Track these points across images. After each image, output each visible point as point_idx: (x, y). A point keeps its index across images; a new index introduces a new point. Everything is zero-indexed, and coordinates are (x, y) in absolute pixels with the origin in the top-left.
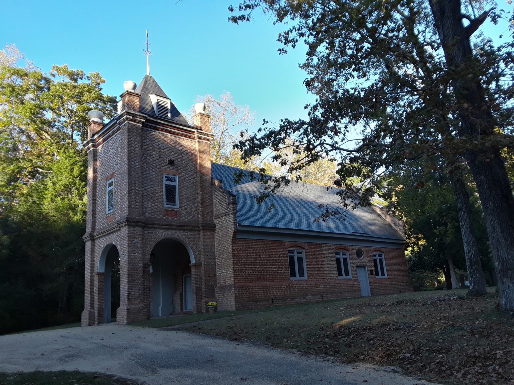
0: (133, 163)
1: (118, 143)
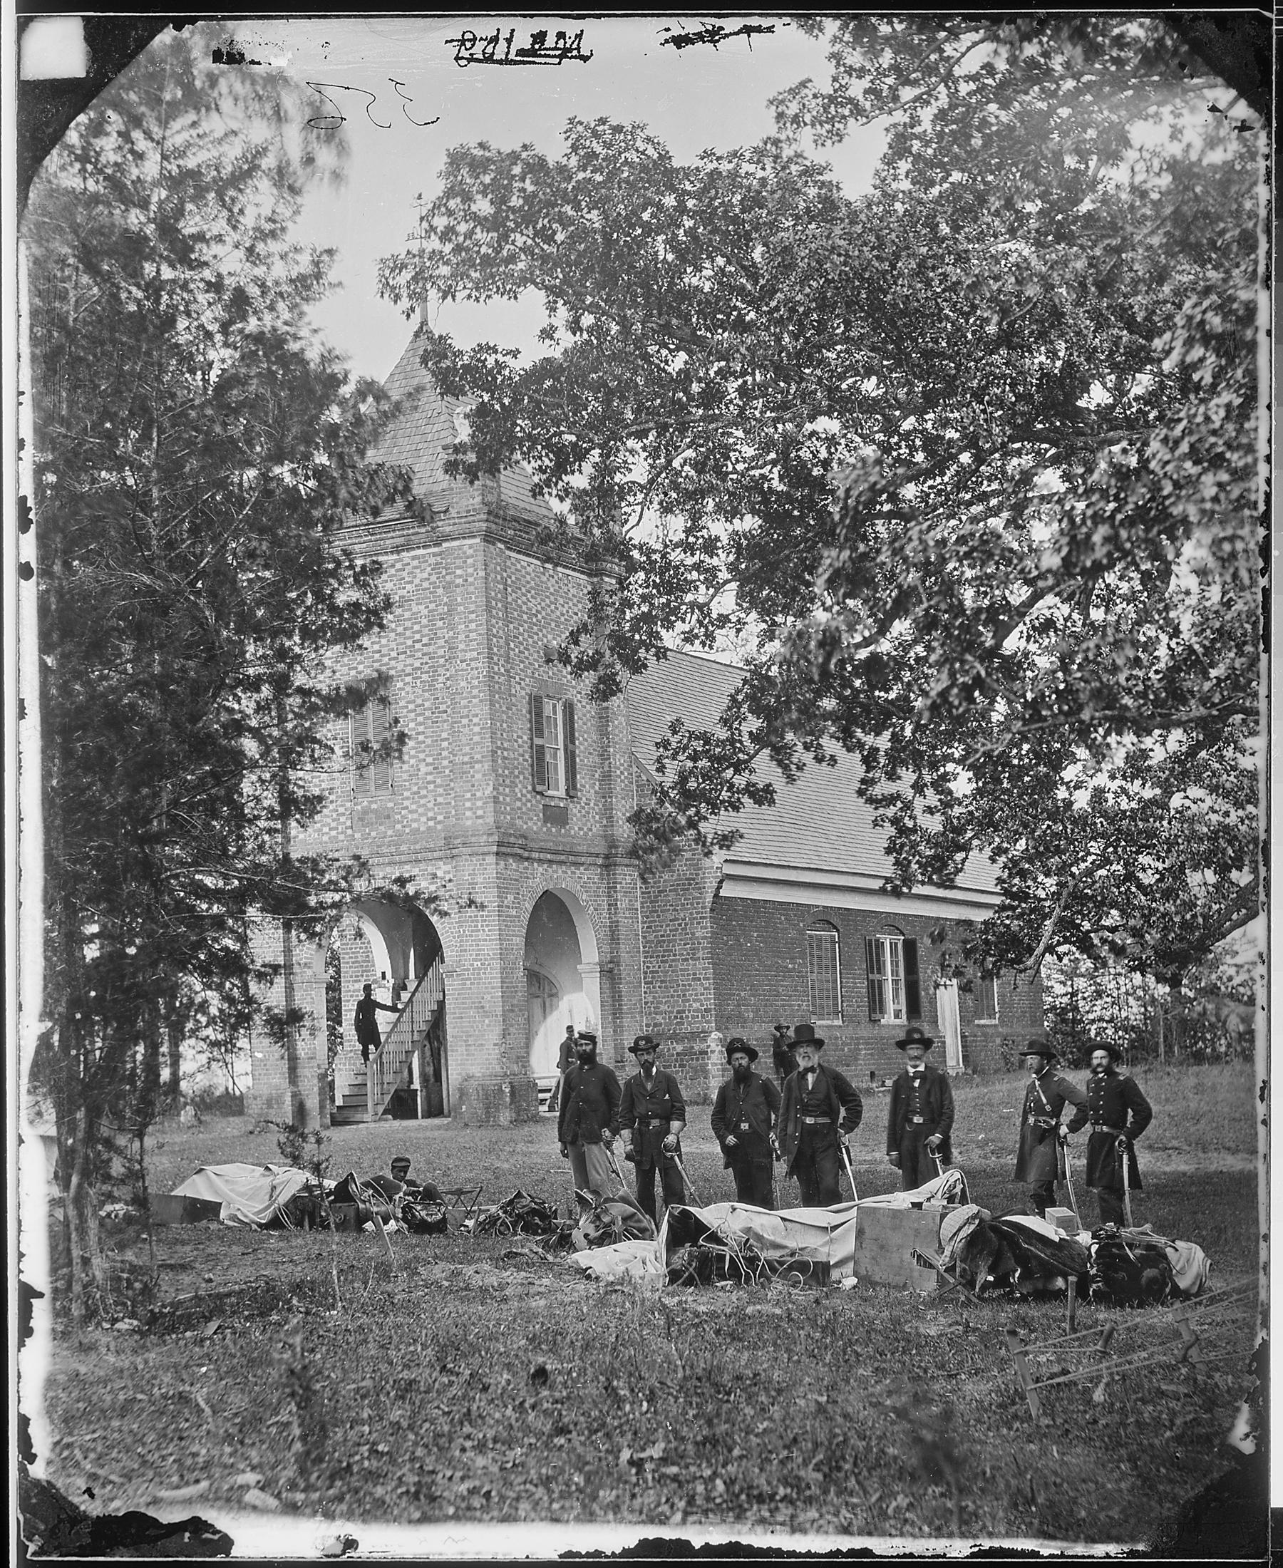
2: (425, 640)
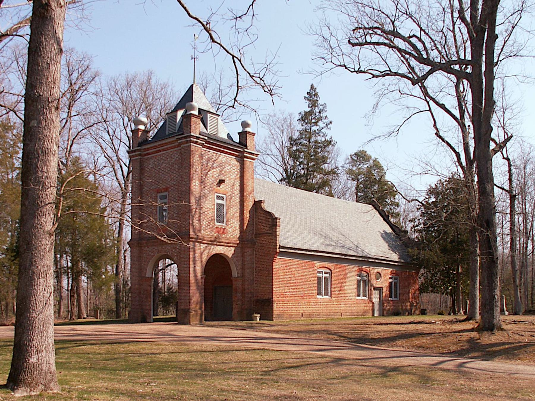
0: (194, 184)
1: (174, 160)
2: (177, 176)
